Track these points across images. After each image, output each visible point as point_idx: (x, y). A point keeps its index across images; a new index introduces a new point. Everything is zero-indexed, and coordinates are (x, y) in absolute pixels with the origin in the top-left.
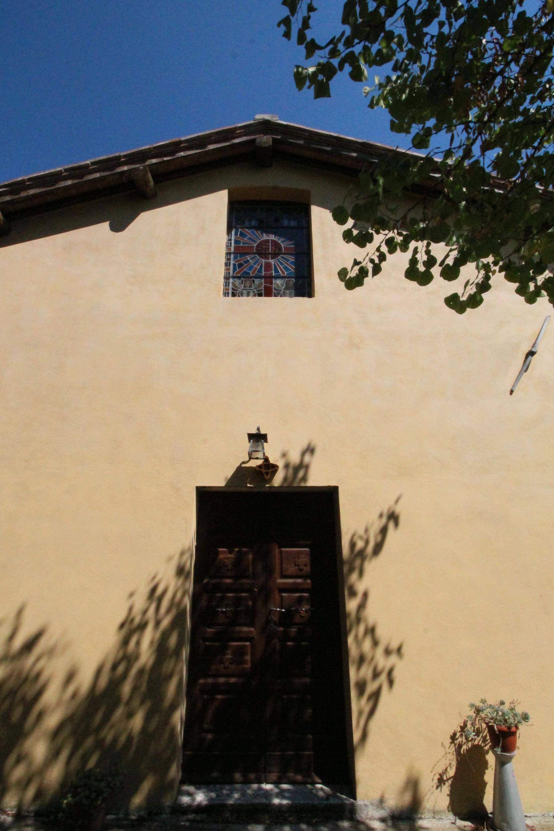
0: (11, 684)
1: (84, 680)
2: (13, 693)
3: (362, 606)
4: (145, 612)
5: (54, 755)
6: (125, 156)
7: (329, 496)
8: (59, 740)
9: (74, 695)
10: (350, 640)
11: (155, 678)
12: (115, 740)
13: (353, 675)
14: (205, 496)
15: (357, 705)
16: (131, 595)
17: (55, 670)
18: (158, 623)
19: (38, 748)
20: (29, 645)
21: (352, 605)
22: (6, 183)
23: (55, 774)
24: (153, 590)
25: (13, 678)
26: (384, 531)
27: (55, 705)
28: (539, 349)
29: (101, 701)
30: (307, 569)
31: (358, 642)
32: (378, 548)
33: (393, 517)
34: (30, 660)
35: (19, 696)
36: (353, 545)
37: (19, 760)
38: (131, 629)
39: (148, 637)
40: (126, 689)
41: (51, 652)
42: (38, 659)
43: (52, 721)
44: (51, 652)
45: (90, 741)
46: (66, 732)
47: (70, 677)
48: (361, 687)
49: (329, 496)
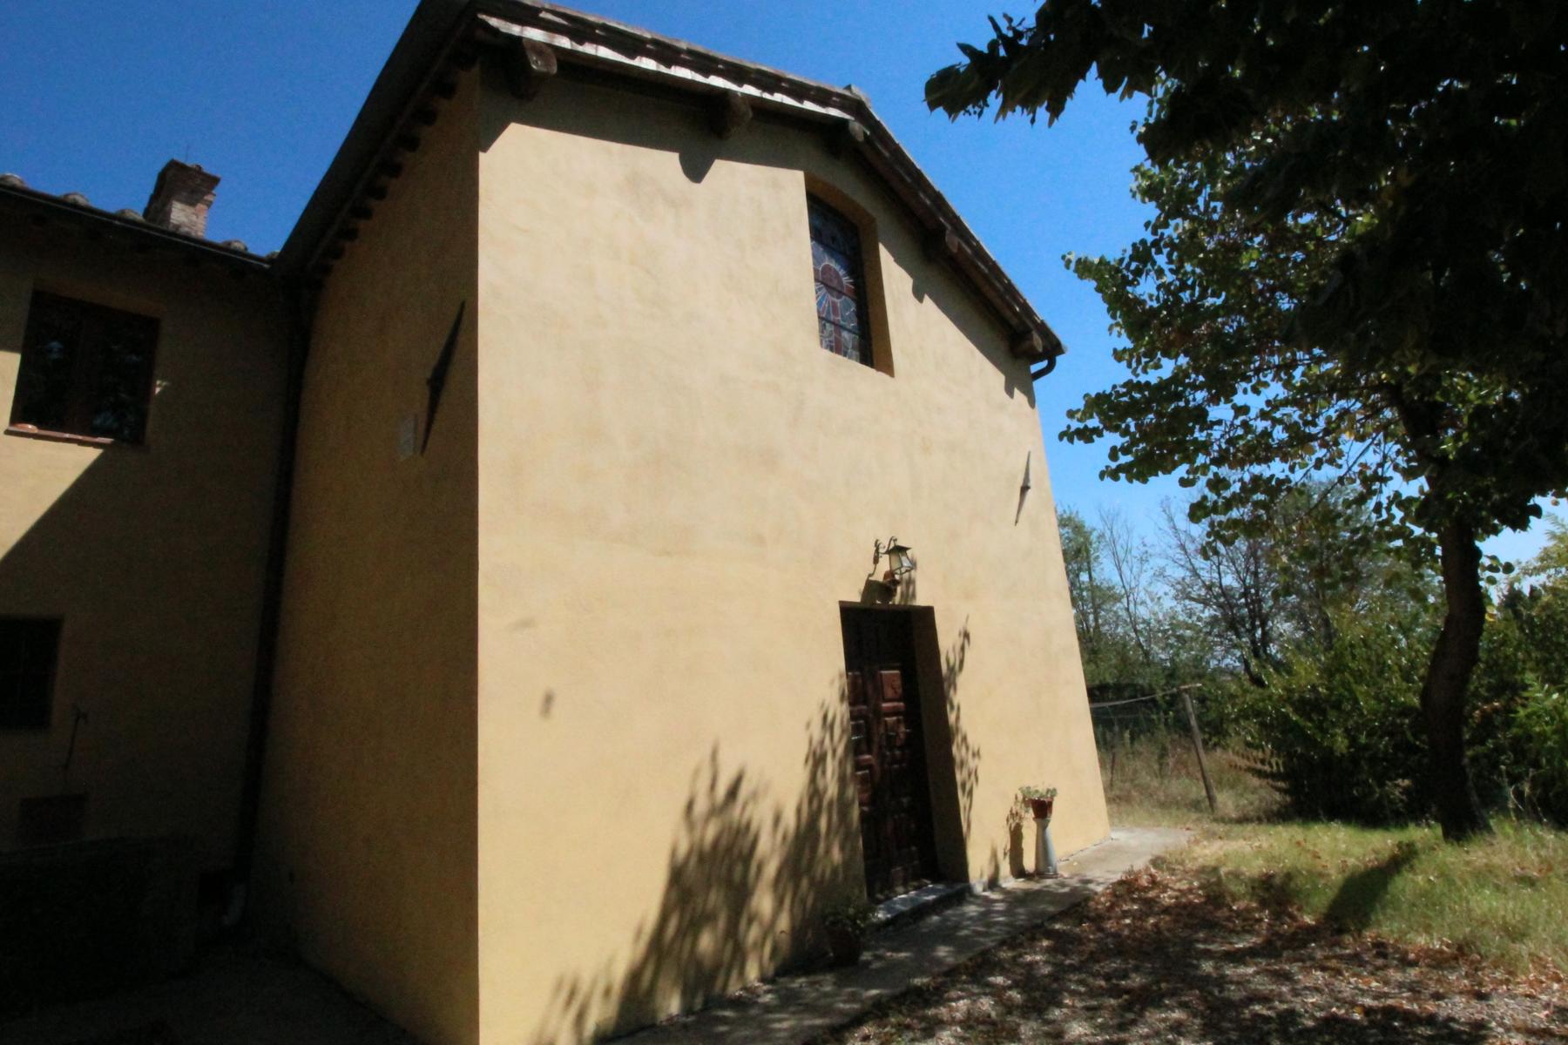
0: (724, 842)
1: (790, 820)
2: (729, 850)
3: (958, 718)
4: (822, 742)
5: (779, 902)
6: (725, 63)
7: (928, 612)
8: (781, 886)
9: (784, 838)
10: (954, 749)
11: (843, 805)
12: (823, 876)
13: (959, 777)
14: (847, 611)
15: (963, 801)
16: (808, 725)
17: (760, 815)
18: (834, 751)
19: (763, 902)
20: (733, 793)
21: (952, 718)
22: (568, 12)
23: (784, 923)
24: (825, 717)
25: (725, 835)
26: (963, 649)
27: (770, 852)
28: (1032, 483)
29: (804, 840)
30: (900, 691)
31: (959, 748)
32: (962, 662)
33: (966, 635)
34: (736, 812)
35: (736, 851)
36: (948, 661)
37: (750, 921)
38: (817, 761)
39: (831, 766)
40: (823, 824)
41: (754, 796)
42: (744, 808)
43: (771, 869)
44: (754, 796)
45: (805, 883)
46: (785, 875)
47: (777, 820)
48: (964, 785)
49: (928, 612)
